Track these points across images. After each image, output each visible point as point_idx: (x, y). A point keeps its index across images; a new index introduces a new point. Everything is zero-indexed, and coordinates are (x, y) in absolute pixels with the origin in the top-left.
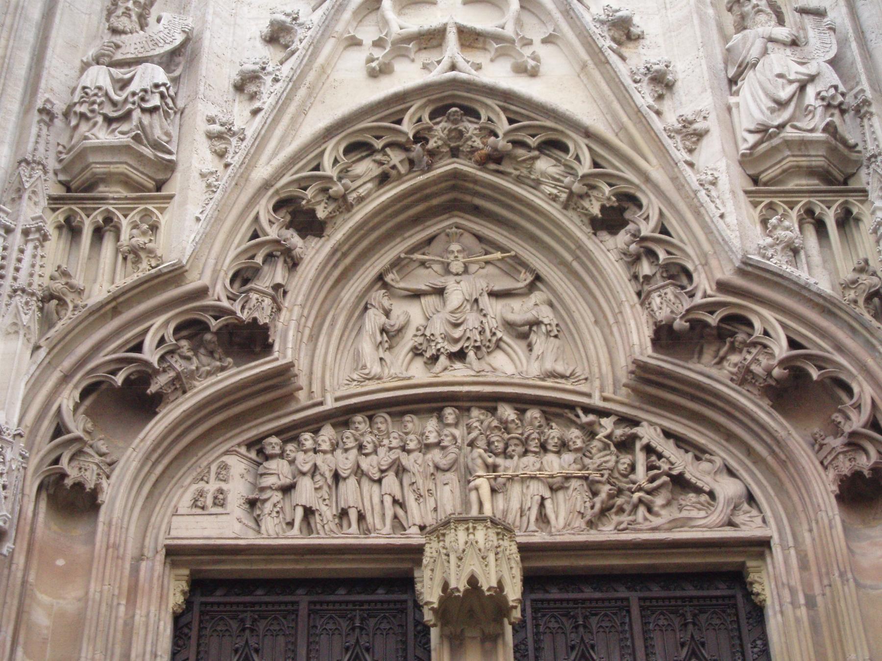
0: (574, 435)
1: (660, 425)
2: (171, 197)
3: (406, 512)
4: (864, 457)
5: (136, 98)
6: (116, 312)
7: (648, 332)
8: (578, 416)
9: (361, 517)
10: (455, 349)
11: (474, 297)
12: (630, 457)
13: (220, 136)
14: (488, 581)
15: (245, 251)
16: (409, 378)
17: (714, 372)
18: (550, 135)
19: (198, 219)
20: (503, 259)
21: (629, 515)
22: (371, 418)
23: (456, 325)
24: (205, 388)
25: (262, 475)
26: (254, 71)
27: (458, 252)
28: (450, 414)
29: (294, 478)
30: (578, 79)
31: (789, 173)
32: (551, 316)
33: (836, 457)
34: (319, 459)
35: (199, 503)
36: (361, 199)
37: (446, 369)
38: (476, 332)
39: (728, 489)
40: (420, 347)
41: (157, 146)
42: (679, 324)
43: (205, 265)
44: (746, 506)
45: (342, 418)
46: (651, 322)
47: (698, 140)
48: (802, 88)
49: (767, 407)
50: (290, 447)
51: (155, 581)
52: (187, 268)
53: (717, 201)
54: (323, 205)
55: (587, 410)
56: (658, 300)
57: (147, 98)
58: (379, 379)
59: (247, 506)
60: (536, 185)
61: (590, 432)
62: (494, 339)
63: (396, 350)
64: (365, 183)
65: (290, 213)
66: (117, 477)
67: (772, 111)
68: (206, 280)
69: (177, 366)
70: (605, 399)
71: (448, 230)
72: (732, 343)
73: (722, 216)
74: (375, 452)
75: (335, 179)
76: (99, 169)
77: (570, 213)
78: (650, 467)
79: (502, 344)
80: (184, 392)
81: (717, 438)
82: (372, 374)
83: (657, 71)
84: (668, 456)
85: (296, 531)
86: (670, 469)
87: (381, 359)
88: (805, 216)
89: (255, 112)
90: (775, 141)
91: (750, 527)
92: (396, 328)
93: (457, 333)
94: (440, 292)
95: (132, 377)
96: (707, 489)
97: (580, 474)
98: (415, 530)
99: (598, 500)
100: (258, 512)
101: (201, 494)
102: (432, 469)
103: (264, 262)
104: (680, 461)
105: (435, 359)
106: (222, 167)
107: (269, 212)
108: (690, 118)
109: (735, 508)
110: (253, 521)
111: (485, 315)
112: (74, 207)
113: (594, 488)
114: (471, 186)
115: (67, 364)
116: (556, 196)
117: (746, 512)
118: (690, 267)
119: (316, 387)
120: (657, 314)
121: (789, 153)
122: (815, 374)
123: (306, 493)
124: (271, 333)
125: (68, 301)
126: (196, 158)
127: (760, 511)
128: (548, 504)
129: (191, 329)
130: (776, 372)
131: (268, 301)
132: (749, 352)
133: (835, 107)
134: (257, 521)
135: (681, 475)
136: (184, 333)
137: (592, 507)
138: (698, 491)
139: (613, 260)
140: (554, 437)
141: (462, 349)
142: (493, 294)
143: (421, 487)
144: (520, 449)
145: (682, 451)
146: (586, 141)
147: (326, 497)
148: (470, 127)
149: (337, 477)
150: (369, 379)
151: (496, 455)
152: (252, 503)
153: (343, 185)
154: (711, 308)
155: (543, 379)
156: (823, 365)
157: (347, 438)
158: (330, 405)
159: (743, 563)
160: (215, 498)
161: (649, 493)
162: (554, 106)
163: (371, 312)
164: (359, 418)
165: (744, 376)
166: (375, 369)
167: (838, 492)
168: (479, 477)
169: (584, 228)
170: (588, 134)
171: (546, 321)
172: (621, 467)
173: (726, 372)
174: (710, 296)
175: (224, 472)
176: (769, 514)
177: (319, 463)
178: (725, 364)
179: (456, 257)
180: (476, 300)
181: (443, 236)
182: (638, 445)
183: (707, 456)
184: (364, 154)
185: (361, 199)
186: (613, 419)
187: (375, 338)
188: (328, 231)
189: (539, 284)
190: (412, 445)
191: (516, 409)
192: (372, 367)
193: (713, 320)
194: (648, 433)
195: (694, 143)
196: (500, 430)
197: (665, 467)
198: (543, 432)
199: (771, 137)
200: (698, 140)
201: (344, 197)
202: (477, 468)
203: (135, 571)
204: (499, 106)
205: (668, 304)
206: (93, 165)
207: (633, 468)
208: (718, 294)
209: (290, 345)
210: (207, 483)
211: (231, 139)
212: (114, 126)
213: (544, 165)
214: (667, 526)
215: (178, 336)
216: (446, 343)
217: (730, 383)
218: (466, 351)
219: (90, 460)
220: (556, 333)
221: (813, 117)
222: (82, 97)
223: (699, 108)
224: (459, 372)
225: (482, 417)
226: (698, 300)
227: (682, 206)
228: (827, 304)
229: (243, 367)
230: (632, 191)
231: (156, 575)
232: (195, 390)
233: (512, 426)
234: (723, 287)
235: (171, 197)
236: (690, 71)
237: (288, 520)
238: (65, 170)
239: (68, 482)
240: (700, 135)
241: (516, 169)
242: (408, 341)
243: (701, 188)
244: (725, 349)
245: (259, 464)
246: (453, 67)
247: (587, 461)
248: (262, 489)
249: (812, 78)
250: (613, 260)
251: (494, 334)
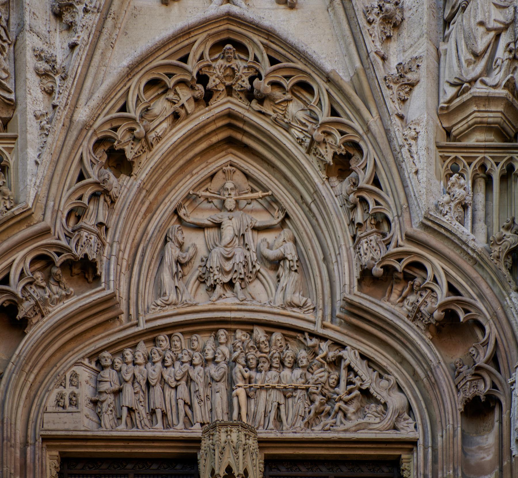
0: (303, 354)
3: (192, 412)
4: (483, 385)
7: (356, 273)
8: (305, 339)
9: (164, 415)
10: (226, 279)
11: (241, 233)
12: (337, 373)
14: (238, 470)
15: (74, 192)
16: (196, 305)
17: (397, 309)
19: (37, 163)
21: (333, 419)
23: (228, 259)
24: (57, 312)
25: (100, 381)
27: (231, 189)
28: (222, 334)
29: (121, 384)
30: (326, 12)
31: (473, 128)
32: (294, 253)
33: (465, 384)
34: (136, 370)
36: (159, 138)
37: (220, 297)
38: (241, 266)
40: (203, 277)
42: (377, 270)
43: (46, 206)
44: (406, 415)
45: (151, 335)
47: (411, 90)
48: (498, 37)
49: (428, 340)
50: (118, 359)
51: (37, 462)
52: (33, 210)
53: (415, 156)
56: (365, 245)
58: (175, 304)
59: (91, 405)
60: (288, 128)
61: (314, 352)
62: (254, 270)
63: (187, 278)
64: (161, 123)
65: (106, 152)
68: (48, 221)
69: (35, 296)
71: (224, 168)
72: (412, 285)
73: (417, 172)
74: (173, 365)
75: (138, 121)
77: (312, 158)
79: (259, 275)
81: (394, 361)
84: (360, 374)
86: (361, 385)
87: (176, 287)
88: (479, 172)
89: (73, 46)
90: (466, 97)
92: (187, 260)
93: (228, 266)
94: (218, 226)
96: (382, 401)
97: (304, 386)
98: (197, 426)
99: (313, 407)
100: (99, 410)
101: (61, 396)
102: (209, 380)
103: (89, 203)
105: (213, 287)
106: (51, 108)
107: (90, 153)
109: (398, 416)
110: (96, 416)
111: (248, 250)
117: (405, 420)
118: (391, 218)
119: (132, 311)
120: (363, 258)
121: (476, 109)
122: (462, 316)
123: (129, 397)
124: (98, 267)
127: (415, 420)
128: (282, 408)
130: (436, 314)
131: (94, 237)
132: (421, 296)
134: (99, 415)
135: (368, 389)
136: (38, 266)
137: (310, 412)
141: (231, 280)
143: (202, 394)
144: (267, 365)
145: (371, 370)
146: (327, 86)
147: (142, 399)
148: (239, 64)
149: (148, 384)
150: (168, 305)
151: (250, 369)
152: (95, 403)
153: (144, 127)
154: (399, 257)
156: (470, 309)
159: (400, 456)
161: (346, 403)
163: (169, 244)
164: (162, 337)
165: (416, 315)
166: (173, 297)
167: (463, 410)
168: (239, 387)
169: (320, 173)
170: (329, 79)
172: (331, 381)
173: (405, 309)
174: (400, 246)
176: (419, 422)
177: (137, 374)
178: (405, 303)
179: (230, 194)
180: (243, 235)
181: (220, 174)
183: (386, 376)
185: (159, 138)
186: (329, 342)
187: (172, 269)
190: (196, 361)
191: (267, 332)
193: (399, 267)
194: (350, 356)
195: (407, 93)
196: (255, 349)
197: (358, 383)
198: (282, 352)
200: (411, 90)
201: (146, 137)
202: (238, 380)
203: (24, 453)
204: (262, 43)
208: (406, 245)
209: (112, 278)
210: (65, 387)
213: (295, 109)
214: (354, 429)
215: (33, 268)
217: (406, 319)
218: (234, 282)
220: (296, 268)
221: (500, 71)
223: (415, 56)
225: (243, 338)
226: (392, 249)
228: (478, 258)
229: (81, 296)
230: (357, 140)
231: (37, 457)
233: (262, 346)
236: (415, 10)
237: (118, 416)
240: (412, 85)
241: (274, 111)
242: (193, 273)
243: (405, 143)
244: (406, 290)
247: (309, 376)
248: (101, 393)
250: (339, 205)
251: (254, 267)
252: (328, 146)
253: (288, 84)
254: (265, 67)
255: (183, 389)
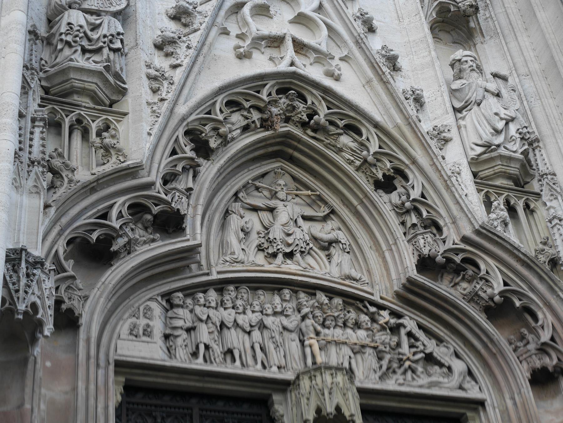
1: (416, 320)
2: (125, 114)
5: (106, 39)
6: (93, 190)
13: (155, 79)
18: (352, 122)
20: (312, 195)
22: (237, 288)
25: (171, 318)
26: (173, 38)
29: (193, 323)
35: (134, 333)
36: (233, 139)
39: (458, 366)
41: (117, 76)
46: (416, 254)
50: (189, 301)
54: (214, 139)
55: (373, 303)
57: (114, 41)
66: (89, 307)
67: (493, 135)
70: (382, 298)
76: (77, 84)
78: (411, 346)
80: (129, 253)
82: (239, 259)
83: (418, 94)
85: (201, 360)
95: (101, 238)
97: (372, 345)
108: (442, 129)
112: (56, 107)
113: (380, 355)
114: (296, 144)
115: (64, 220)
116: (352, 161)
125: (64, 175)
126: (138, 90)
129: (137, 209)
133: (526, 140)
137: (381, 367)
138: (441, 365)
139: (388, 210)
140: (353, 319)
142: (305, 218)
146: (375, 130)
148: (301, 106)
155: (344, 280)
157: (227, 300)
158: (215, 276)
160: (145, 330)
162: (357, 104)
168: (311, 338)
171: (343, 241)
175: (149, 313)
178: (458, 287)
182: (403, 332)
184: (235, 109)
188: (213, 157)
189: (332, 216)
192: (239, 255)
199: (492, 151)
202: (309, 332)
206: (73, 80)
207: (399, 345)
211: (164, 82)
212: (87, 55)
216: (283, 246)
219: (75, 293)
222: (68, 30)
224: (291, 266)
227: (439, 184)
232: (137, 253)
234: (465, 240)
235: (125, 114)
238: (47, 79)
239: (64, 307)
245: (167, 311)
246: (292, 64)
249: (513, 119)
252: (378, 167)
253: (341, 123)
254: (323, 111)
255: (256, 334)
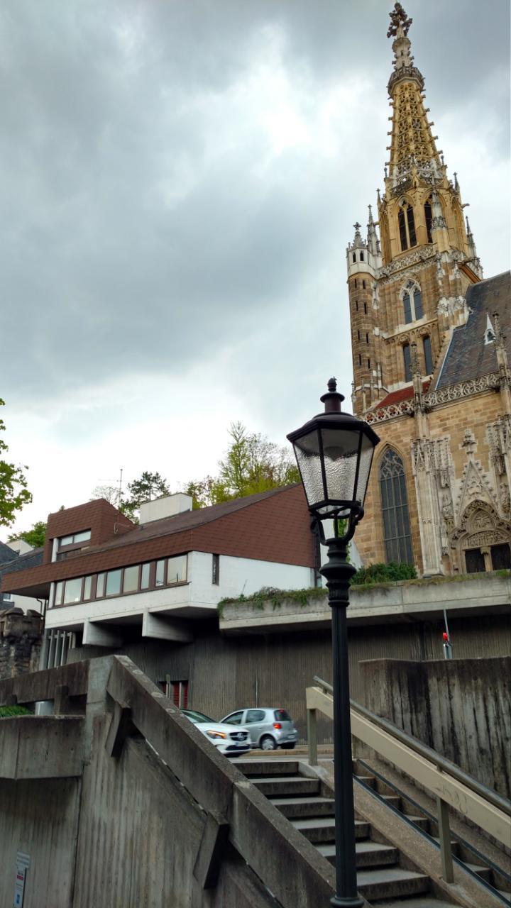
91: (508, 541)
104: (502, 535)
126: (455, 515)
205: (498, 522)
